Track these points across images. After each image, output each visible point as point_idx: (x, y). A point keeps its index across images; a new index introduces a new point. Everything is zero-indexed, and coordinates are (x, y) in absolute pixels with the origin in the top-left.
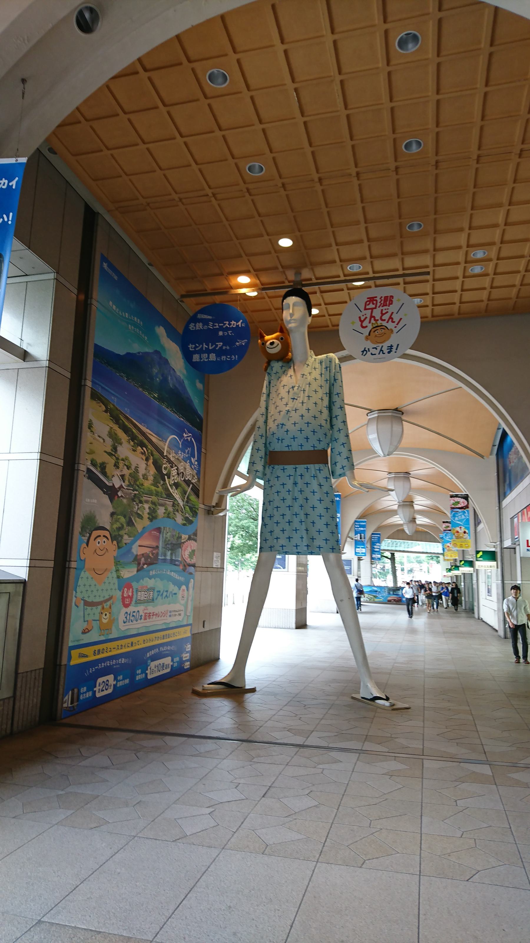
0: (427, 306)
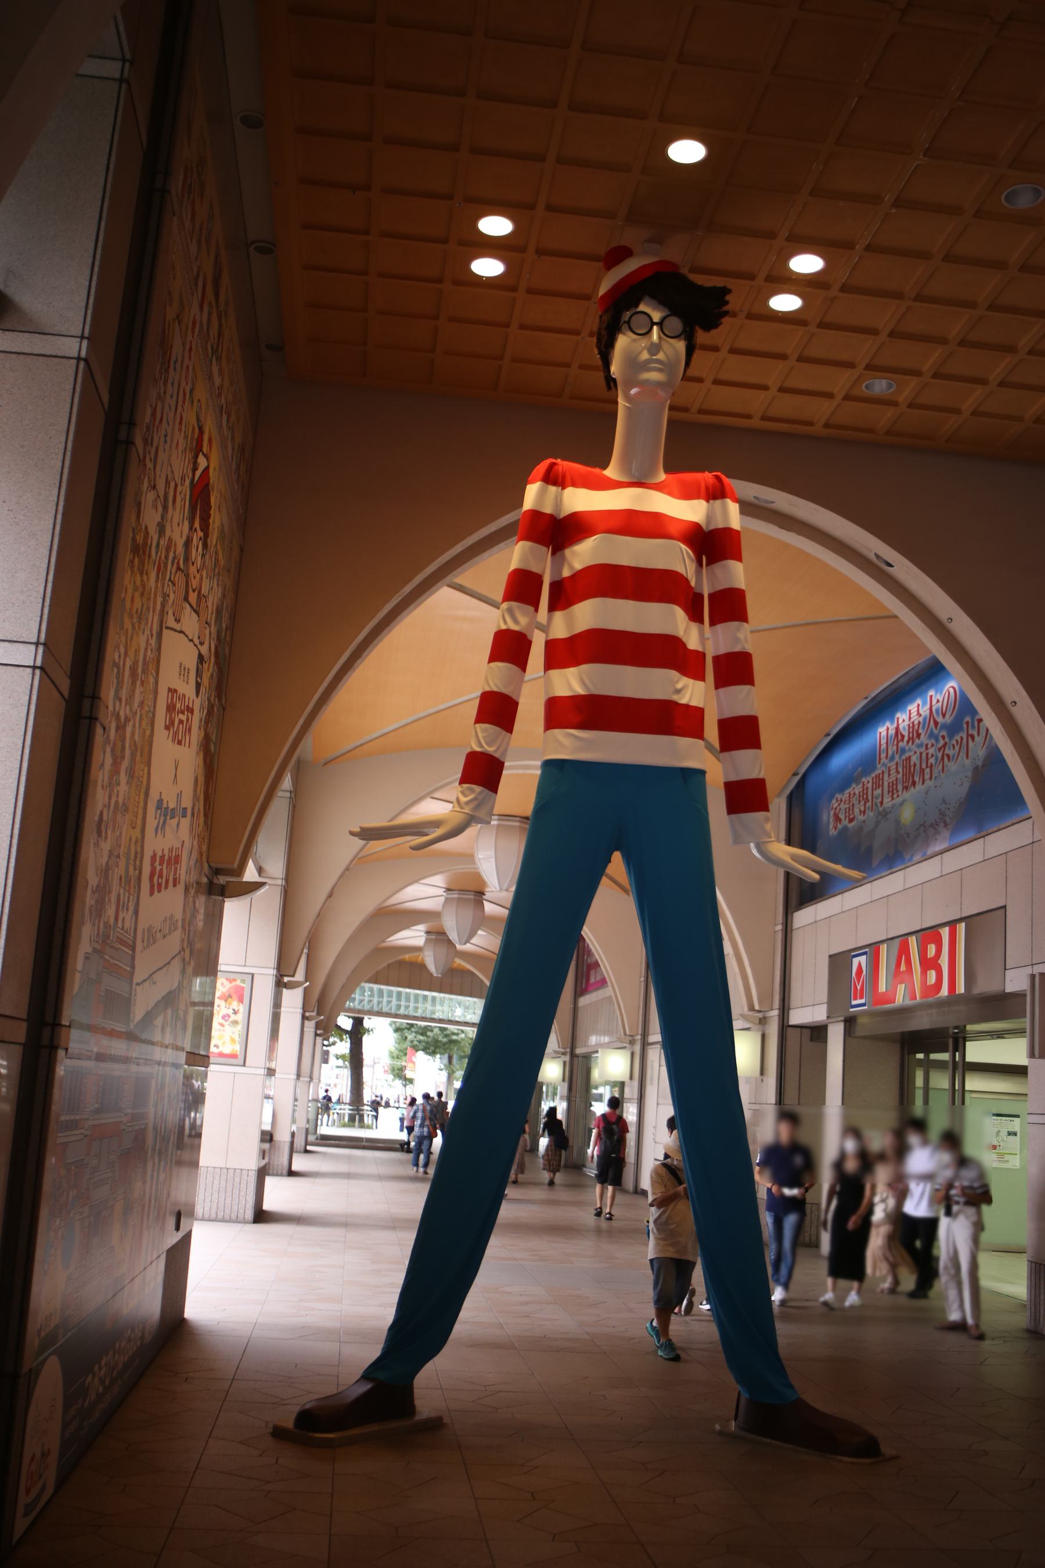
0: (894, 404)
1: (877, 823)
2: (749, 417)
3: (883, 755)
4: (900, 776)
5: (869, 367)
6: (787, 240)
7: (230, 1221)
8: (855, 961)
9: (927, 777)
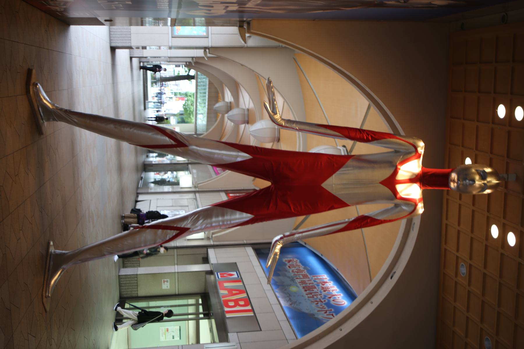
0: (456, 276)
1: (289, 277)
2: (447, 219)
3: (316, 278)
4: (308, 285)
5: (470, 265)
6: (521, 232)
7: (110, 37)
8: (235, 273)
9: (309, 296)
